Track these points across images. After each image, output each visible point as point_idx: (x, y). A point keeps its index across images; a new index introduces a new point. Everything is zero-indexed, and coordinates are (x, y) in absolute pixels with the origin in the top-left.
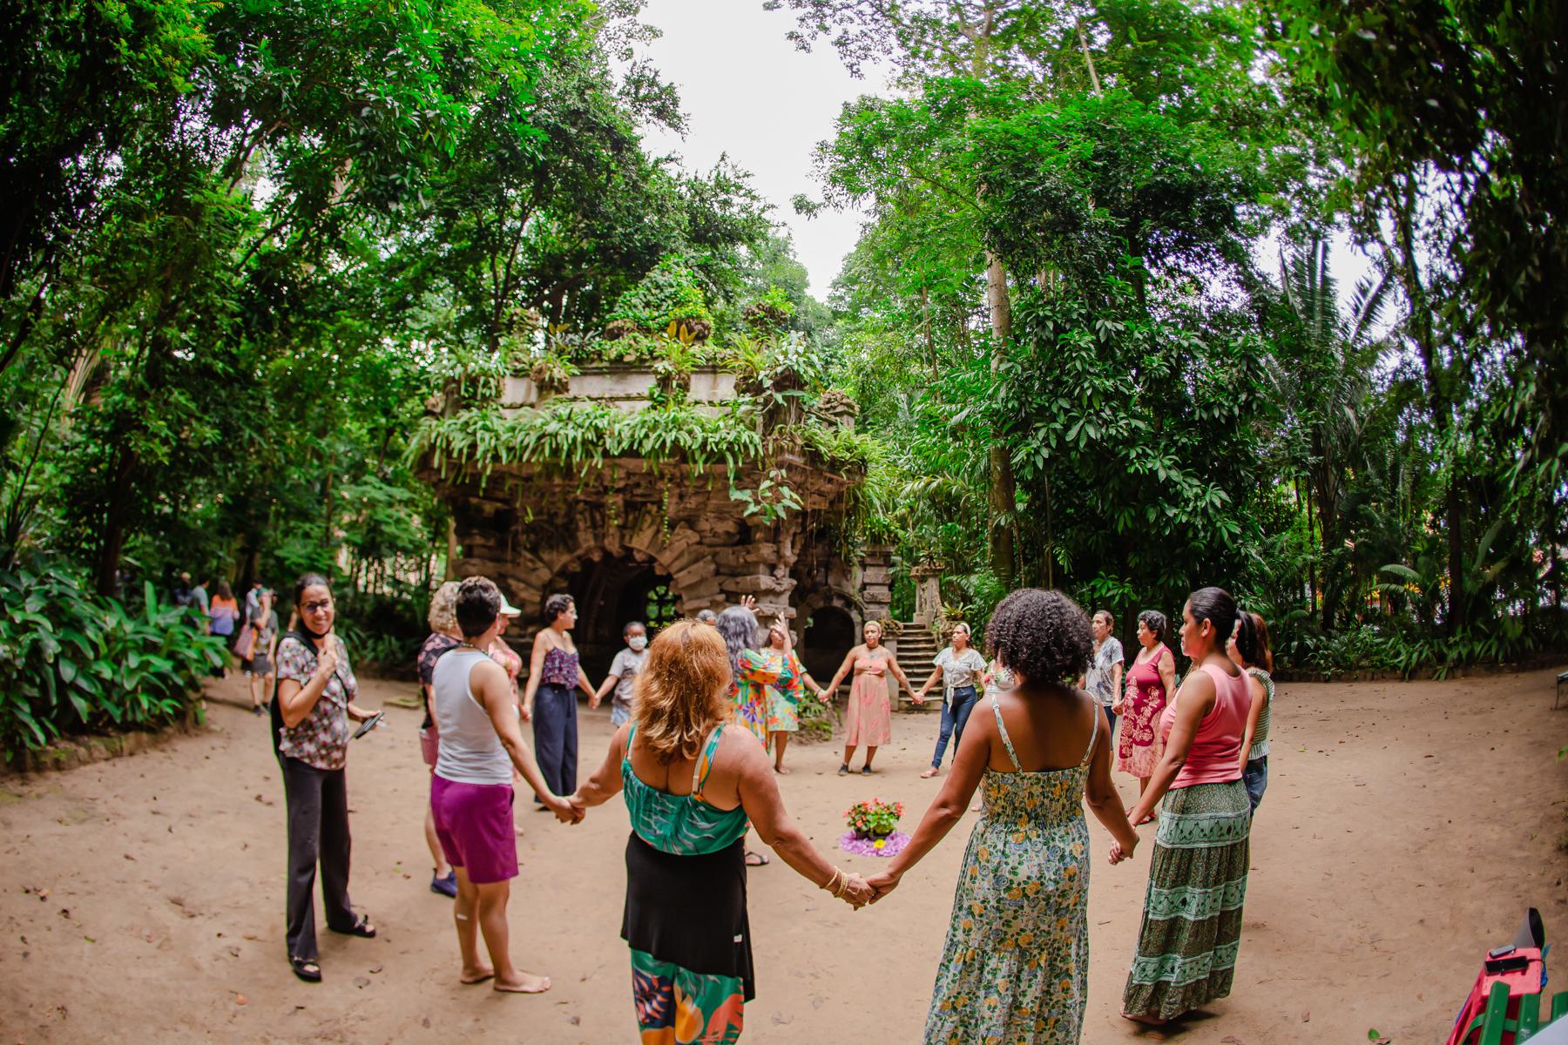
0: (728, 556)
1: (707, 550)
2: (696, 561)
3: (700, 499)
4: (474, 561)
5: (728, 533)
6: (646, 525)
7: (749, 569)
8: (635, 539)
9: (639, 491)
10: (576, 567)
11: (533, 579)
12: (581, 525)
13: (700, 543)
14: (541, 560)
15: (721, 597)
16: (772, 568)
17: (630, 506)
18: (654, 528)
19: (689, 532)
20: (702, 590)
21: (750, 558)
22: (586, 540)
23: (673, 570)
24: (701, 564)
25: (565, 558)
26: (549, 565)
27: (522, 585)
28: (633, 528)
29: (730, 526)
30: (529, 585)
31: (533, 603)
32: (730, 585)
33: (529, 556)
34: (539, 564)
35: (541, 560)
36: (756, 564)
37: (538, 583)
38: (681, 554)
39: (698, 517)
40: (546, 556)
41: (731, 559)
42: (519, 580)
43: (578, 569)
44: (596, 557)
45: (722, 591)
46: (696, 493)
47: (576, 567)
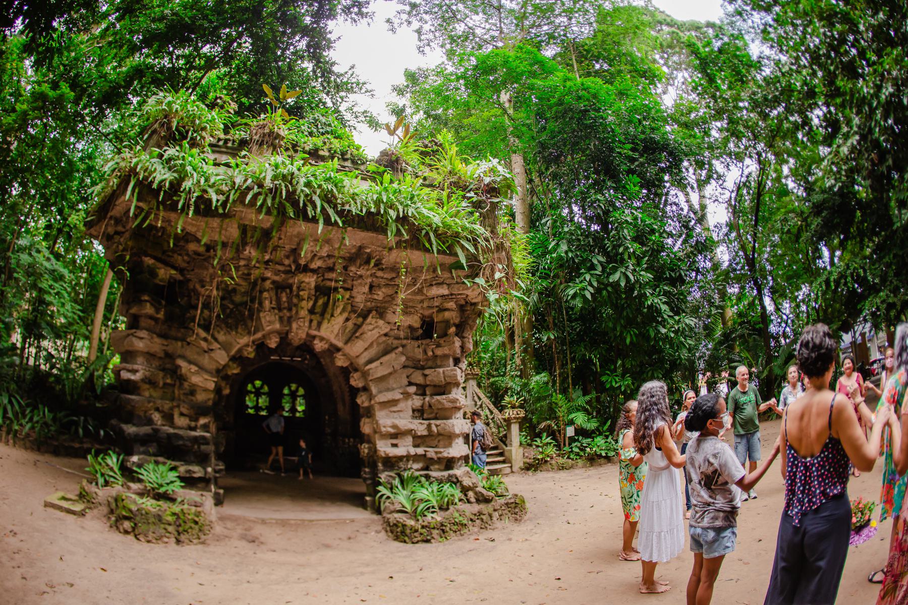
0: (416, 350)
1: (396, 342)
2: (386, 352)
3: (389, 291)
4: (143, 334)
5: (410, 327)
6: (339, 310)
7: (436, 362)
8: (325, 325)
9: (333, 275)
10: (250, 352)
11: (205, 361)
12: (267, 304)
13: (386, 335)
14: (216, 340)
15: (412, 389)
16: (457, 361)
17: (323, 291)
18: (345, 315)
19: (381, 322)
20: (392, 382)
21: (439, 352)
22: (270, 322)
23: (362, 360)
24: (393, 355)
25: (244, 340)
26: (225, 347)
27: (194, 368)
28: (322, 314)
29: (414, 321)
30: (201, 368)
31: (206, 390)
32: (418, 378)
33: (203, 334)
34: (216, 345)
35: (216, 340)
36: (446, 357)
37: (212, 367)
38: (371, 345)
39: (386, 308)
40: (221, 337)
41: (419, 354)
42: (190, 362)
43: (252, 356)
44: (273, 343)
45: (410, 384)
46: (387, 285)
47: (250, 352)
